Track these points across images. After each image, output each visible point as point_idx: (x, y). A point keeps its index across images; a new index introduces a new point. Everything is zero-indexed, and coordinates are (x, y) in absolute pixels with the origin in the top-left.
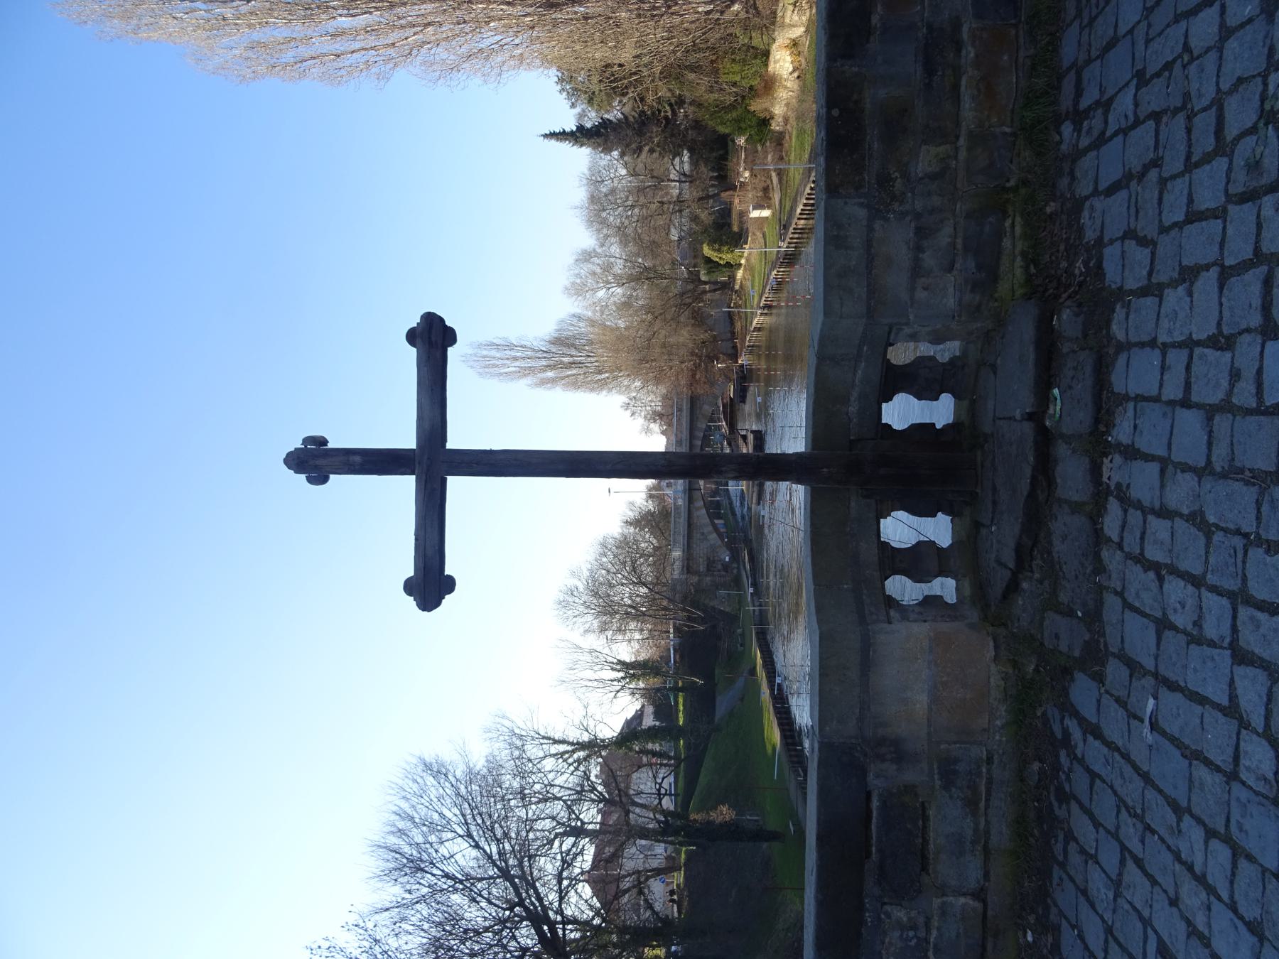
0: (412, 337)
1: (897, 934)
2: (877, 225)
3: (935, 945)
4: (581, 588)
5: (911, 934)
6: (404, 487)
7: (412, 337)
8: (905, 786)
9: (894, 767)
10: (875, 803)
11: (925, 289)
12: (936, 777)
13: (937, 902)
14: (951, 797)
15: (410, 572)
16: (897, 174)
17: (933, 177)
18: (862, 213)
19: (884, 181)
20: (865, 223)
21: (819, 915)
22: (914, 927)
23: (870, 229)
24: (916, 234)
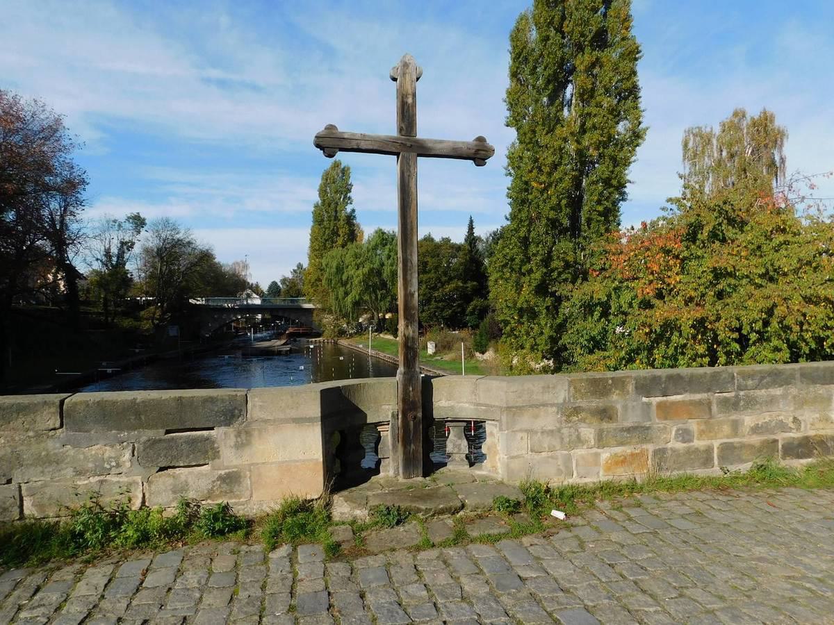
0: (481, 140)
1: (113, 455)
2: (554, 409)
3: (106, 481)
4: (178, 236)
5: (114, 464)
6: (388, 127)
7: (481, 140)
8: (219, 452)
9: (232, 444)
10: (205, 433)
11: (522, 438)
12: (227, 471)
13: (139, 479)
14: (214, 482)
15: (340, 129)
16: (580, 417)
17: (578, 437)
18: (561, 400)
19: (577, 410)
20: (556, 402)
21: (114, 403)
22: (118, 465)
23: (552, 405)
24: (550, 430)
